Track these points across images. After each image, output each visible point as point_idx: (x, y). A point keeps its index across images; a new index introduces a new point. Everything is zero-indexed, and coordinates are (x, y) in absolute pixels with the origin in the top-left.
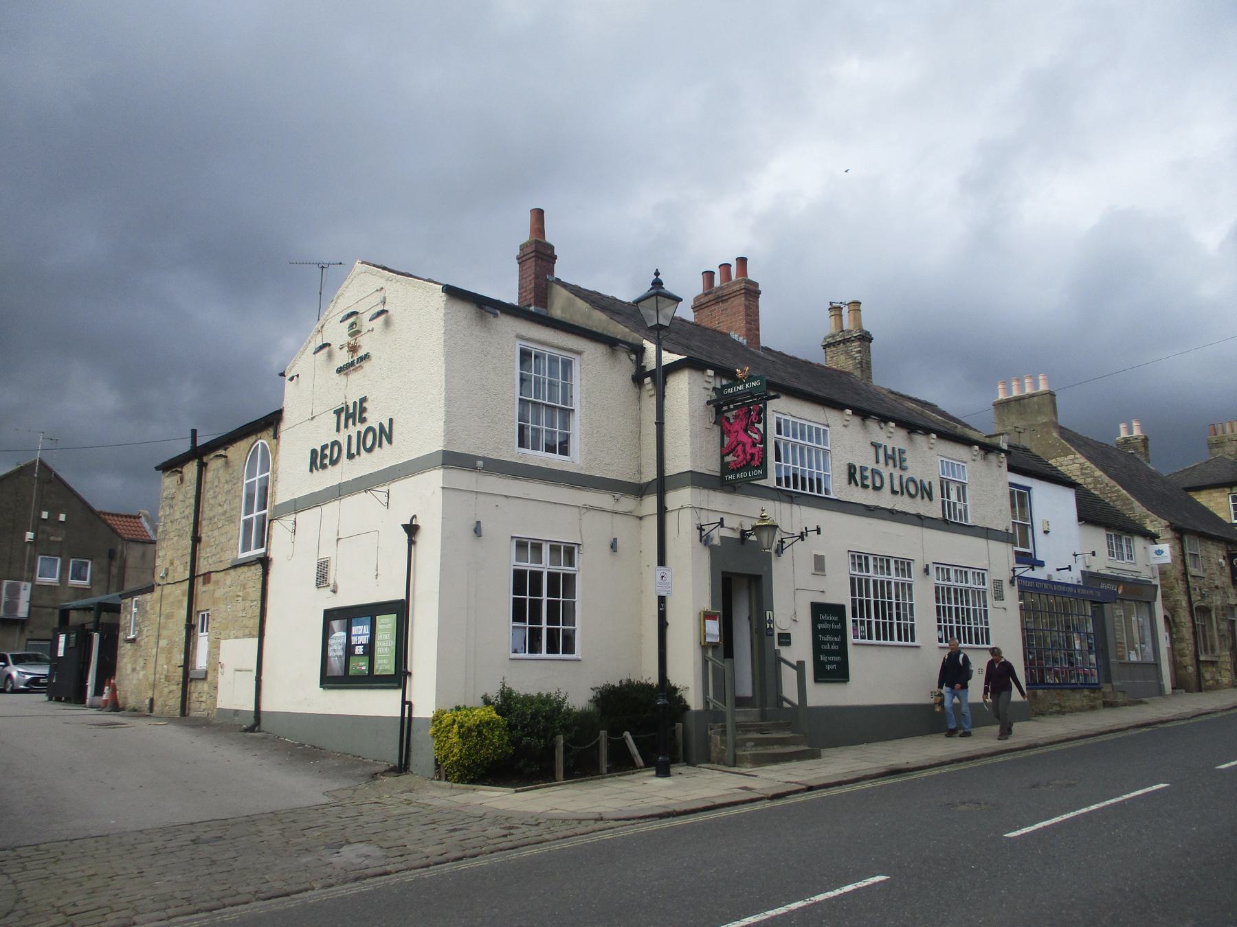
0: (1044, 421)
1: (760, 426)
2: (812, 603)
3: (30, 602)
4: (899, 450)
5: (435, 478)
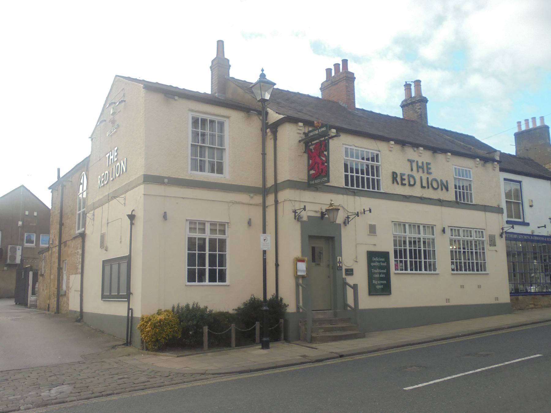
0: (543, 143)
1: (326, 153)
2: (367, 251)
3: (22, 256)
4: (427, 163)
5: (141, 189)
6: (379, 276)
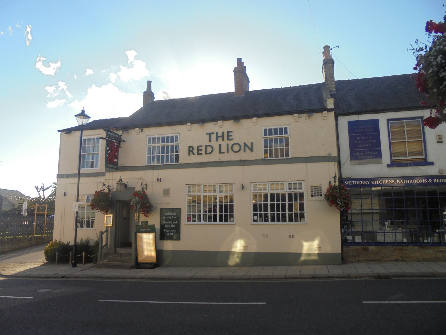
6: (170, 226)
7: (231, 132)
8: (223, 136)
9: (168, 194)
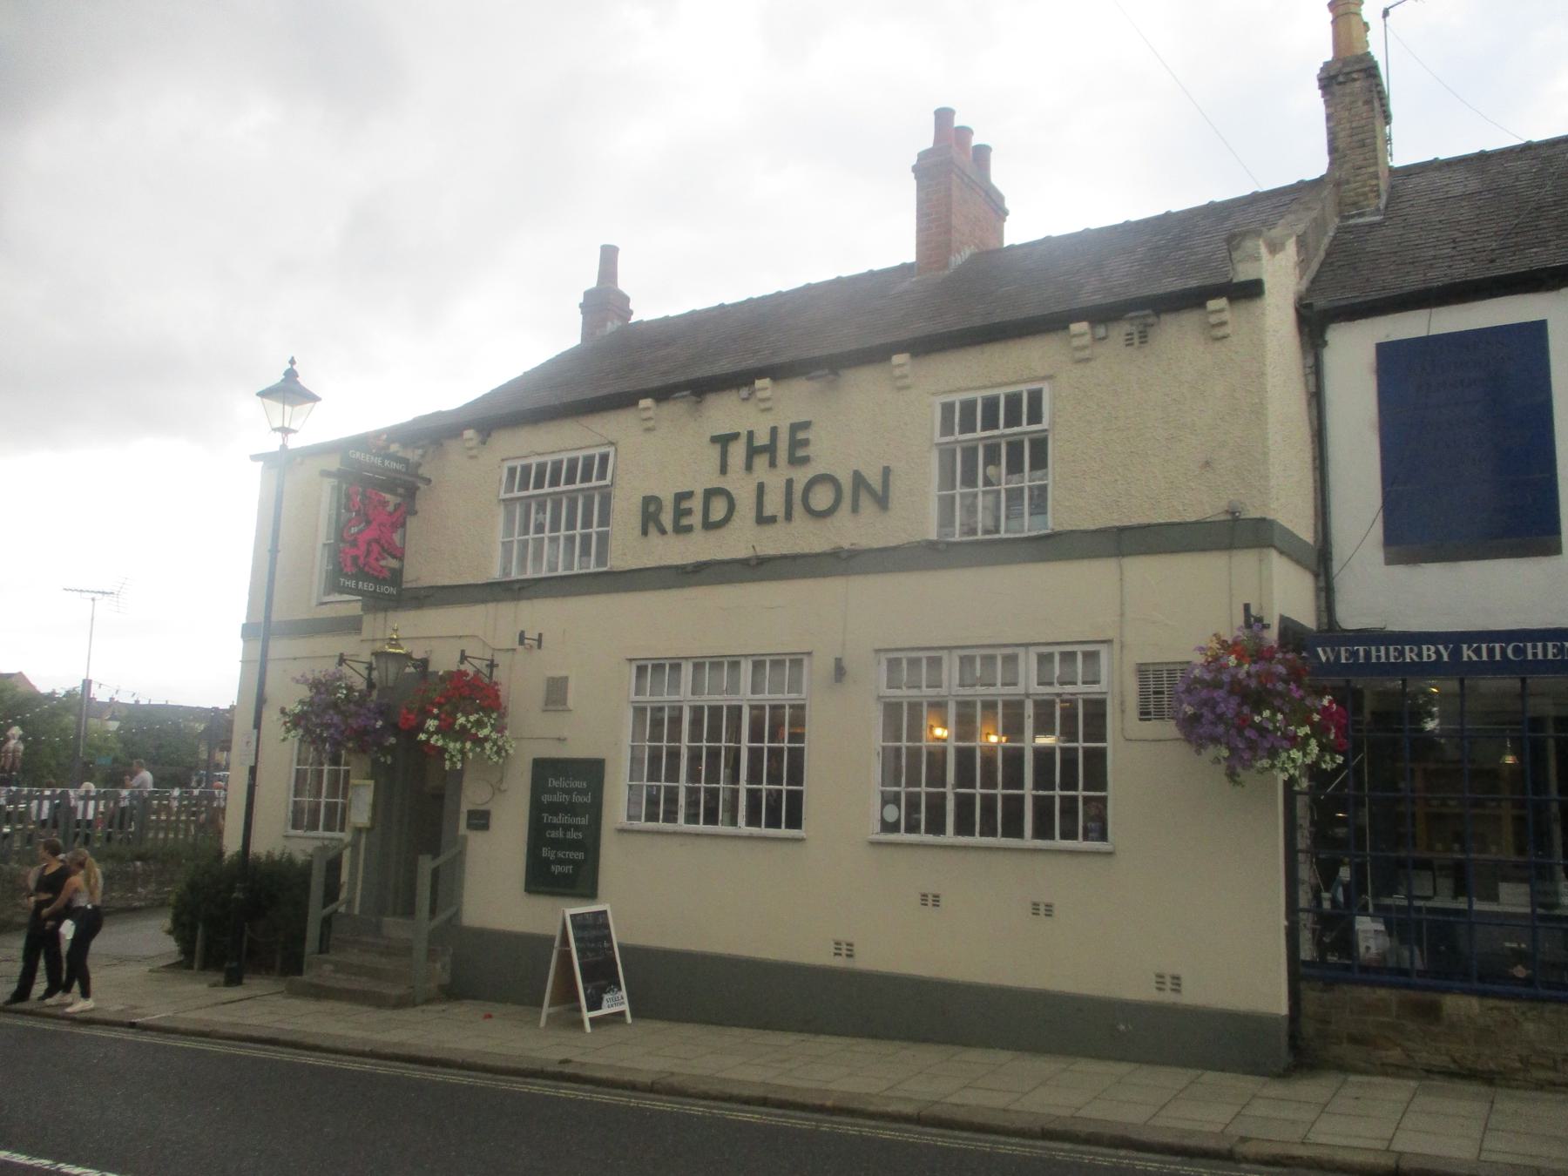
6: (565, 835)
7: (806, 425)
8: (770, 449)
9: (563, 700)
